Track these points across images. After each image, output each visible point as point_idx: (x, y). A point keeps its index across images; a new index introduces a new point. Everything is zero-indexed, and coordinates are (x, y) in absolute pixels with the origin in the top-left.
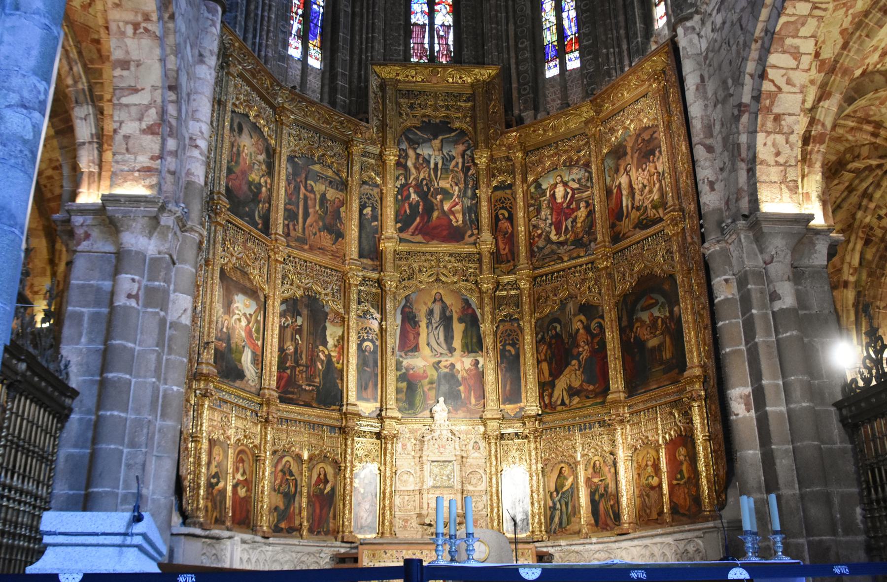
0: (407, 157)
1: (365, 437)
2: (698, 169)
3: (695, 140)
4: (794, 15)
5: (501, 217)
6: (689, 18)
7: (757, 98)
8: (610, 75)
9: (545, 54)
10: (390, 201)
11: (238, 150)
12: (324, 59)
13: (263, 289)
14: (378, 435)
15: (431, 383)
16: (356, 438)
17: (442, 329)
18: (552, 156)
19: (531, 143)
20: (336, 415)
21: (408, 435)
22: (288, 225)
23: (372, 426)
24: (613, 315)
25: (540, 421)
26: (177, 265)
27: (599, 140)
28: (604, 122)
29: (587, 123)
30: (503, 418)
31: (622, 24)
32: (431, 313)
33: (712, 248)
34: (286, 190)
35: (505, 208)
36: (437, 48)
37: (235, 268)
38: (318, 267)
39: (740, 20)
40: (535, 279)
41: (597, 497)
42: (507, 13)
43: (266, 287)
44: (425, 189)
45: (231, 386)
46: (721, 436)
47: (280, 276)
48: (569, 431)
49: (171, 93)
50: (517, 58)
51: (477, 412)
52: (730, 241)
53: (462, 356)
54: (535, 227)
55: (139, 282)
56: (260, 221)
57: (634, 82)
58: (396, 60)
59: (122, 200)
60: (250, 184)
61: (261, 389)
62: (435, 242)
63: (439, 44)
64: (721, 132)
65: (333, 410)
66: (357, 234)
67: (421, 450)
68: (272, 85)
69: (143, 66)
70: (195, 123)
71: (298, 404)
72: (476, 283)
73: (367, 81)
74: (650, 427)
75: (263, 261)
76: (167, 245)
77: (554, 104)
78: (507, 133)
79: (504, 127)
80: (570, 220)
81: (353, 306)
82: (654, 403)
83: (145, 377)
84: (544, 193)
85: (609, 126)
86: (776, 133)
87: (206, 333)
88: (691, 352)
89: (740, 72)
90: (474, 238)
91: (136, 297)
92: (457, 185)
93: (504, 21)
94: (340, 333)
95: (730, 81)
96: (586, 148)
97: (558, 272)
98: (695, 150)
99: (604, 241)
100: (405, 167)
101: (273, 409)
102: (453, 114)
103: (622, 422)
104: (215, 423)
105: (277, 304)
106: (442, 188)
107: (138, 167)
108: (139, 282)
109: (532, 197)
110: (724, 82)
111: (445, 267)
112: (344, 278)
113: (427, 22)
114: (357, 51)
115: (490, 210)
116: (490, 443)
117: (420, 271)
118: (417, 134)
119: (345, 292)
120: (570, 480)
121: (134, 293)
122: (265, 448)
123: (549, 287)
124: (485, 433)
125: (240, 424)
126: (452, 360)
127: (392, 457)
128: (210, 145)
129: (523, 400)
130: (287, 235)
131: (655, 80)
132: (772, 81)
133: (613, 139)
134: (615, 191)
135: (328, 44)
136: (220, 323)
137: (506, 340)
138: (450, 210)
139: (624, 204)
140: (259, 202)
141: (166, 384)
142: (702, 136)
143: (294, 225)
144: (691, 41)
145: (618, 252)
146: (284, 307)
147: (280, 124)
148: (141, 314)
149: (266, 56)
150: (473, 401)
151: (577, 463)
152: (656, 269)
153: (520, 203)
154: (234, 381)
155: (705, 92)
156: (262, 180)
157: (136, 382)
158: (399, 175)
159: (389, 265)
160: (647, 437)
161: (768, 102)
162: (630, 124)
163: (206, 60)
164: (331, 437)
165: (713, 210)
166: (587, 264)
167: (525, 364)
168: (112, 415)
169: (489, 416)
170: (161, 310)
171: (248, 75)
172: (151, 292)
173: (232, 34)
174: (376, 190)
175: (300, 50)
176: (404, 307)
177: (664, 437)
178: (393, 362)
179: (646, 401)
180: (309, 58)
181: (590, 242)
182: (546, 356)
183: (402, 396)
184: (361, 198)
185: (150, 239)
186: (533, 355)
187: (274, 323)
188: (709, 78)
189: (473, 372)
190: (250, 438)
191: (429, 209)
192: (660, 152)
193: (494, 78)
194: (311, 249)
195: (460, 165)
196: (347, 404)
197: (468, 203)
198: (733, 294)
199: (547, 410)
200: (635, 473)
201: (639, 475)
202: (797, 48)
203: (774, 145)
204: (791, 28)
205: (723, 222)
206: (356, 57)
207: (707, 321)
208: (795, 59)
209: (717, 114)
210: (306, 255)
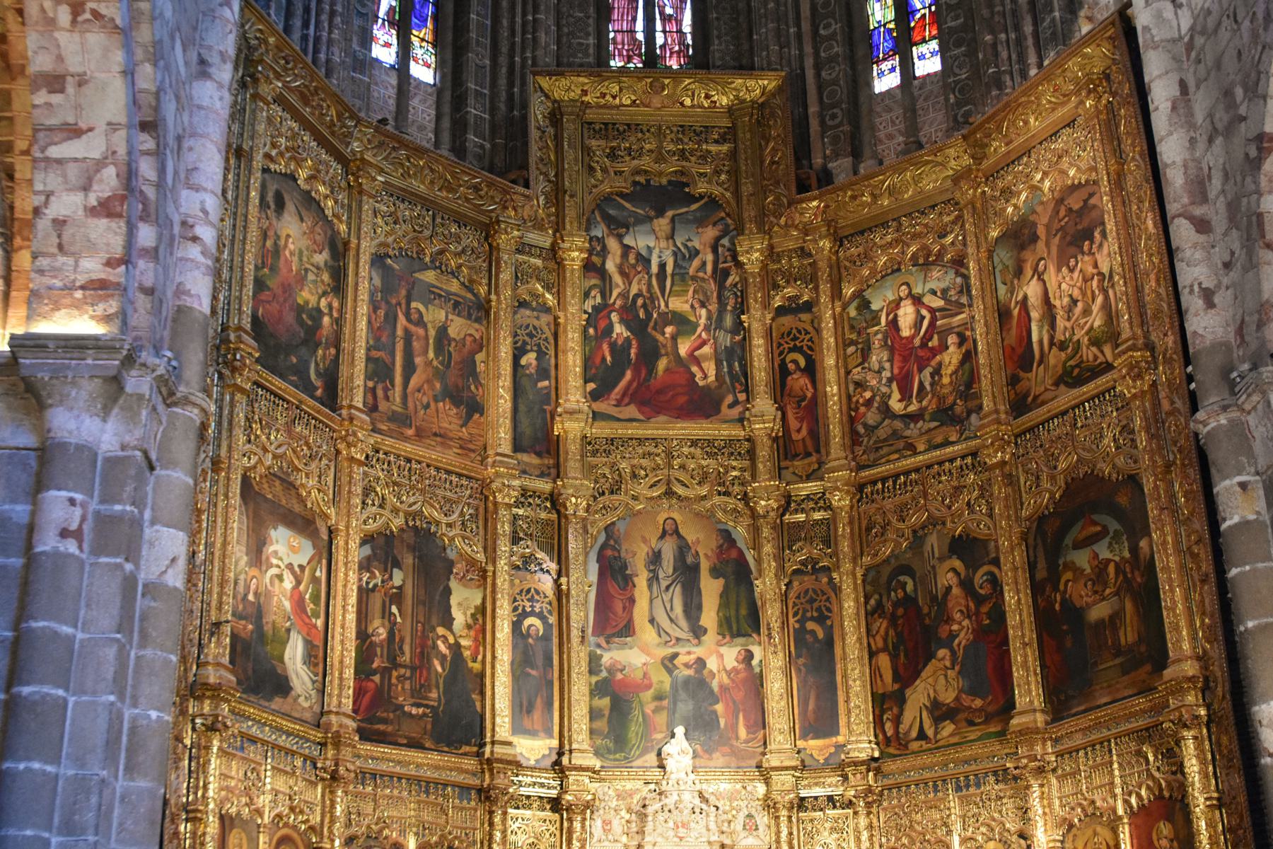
0: (604, 252)
1: (529, 807)
2: (1179, 266)
3: (1172, 208)
5: (791, 366)
8: (1000, 86)
9: (872, 48)
10: (572, 339)
11: (275, 244)
12: (440, 66)
13: (326, 517)
14: (555, 804)
15: (659, 697)
16: (510, 810)
17: (678, 589)
18: (890, 245)
19: (846, 221)
20: (470, 763)
21: (614, 804)
22: (373, 390)
23: (542, 785)
24: (1019, 556)
25: (878, 771)
27: (983, 211)
28: (991, 176)
29: (957, 179)
30: (804, 767)
33: (1211, 421)
34: (369, 322)
35: (799, 350)
36: (660, 39)
37: (271, 476)
38: (433, 472)
40: (861, 488)
43: (332, 512)
44: (642, 314)
45: (263, 709)
46: (1242, 799)
47: (359, 491)
48: (936, 790)
49: (144, 137)
50: (816, 54)
51: (752, 755)
52: (1247, 407)
53: (719, 644)
54: (860, 385)
55: (84, 505)
56: (318, 383)
57: (1048, 98)
58: (581, 65)
59: (51, 345)
60: (300, 309)
61: (322, 714)
62: (662, 418)
63: (664, 31)
65: (465, 754)
66: (509, 405)
67: (641, 832)
68: (340, 116)
69: (91, 85)
70: (193, 194)
72: (745, 498)
73: (525, 106)
75: (325, 461)
76: (138, 433)
77: (892, 144)
78: (802, 201)
79: (794, 189)
80: (927, 372)
81: (504, 546)
82: (1105, 733)
83: (94, 693)
85: (1000, 184)
87: (214, 603)
88: (1177, 629)
89: (1259, 73)
90: (739, 409)
91: (78, 535)
92: (703, 305)
94: (478, 602)
95: (1239, 92)
96: (957, 228)
97: (907, 473)
98: (1172, 229)
99: (997, 411)
100: (602, 273)
101: (346, 753)
102: (694, 167)
103: (1040, 771)
104: (233, 783)
105: (353, 545)
106: (674, 313)
107: (81, 279)
108: (84, 505)
109: (852, 327)
110: (1228, 93)
111: (683, 467)
112: (483, 491)
114: (505, 49)
115: (770, 353)
116: (777, 818)
117: (634, 476)
118: (623, 208)
119: (486, 520)
121: (74, 526)
122: (331, 832)
123: (888, 504)
124: (767, 797)
125: (282, 784)
126: (699, 651)
128: (221, 235)
129: (843, 730)
130: (372, 409)
131: (1089, 92)
133: (1010, 210)
134: (1016, 312)
135: (449, 36)
136: (241, 583)
137: (805, 611)
138: (691, 354)
139: (1035, 337)
140: (318, 345)
141: (135, 705)
142: (1186, 200)
143: (386, 390)
144: (1159, 16)
145: (1024, 433)
146: (367, 550)
147: (355, 191)
148: (87, 568)
149: (328, 61)
150: (743, 732)
152: (1100, 465)
153: (829, 339)
154: (270, 700)
155: (1190, 114)
156: (323, 302)
157: (76, 703)
158: (591, 288)
159: (572, 466)
160: (1093, 802)
162: (1042, 179)
163: (212, 70)
164: (462, 809)
166: (963, 457)
167: (844, 658)
168: (28, 770)
169: (775, 763)
170: (127, 560)
171: (293, 99)
172: (105, 523)
173: (261, 19)
174: (545, 319)
175: (394, 49)
176: (603, 547)
177: (1126, 802)
178: (584, 656)
179: (1088, 728)
180: (412, 63)
181: (969, 413)
182: (885, 640)
183: (602, 724)
184: (516, 335)
185: (104, 420)
186: (859, 639)
187: (348, 582)
188: (1198, 87)
190: (302, 812)
191: (650, 353)
192: (1104, 234)
193: (773, 95)
194: (420, 435)
195: (709, 268)
196: (493, 743)
197: (726, 340)
198: (1258, 513)
199: (891, 750)
205: (1232, 370)
206: (503, 60)
207: (1207, 566)
209: (1215, 157)
210: (408, 448)
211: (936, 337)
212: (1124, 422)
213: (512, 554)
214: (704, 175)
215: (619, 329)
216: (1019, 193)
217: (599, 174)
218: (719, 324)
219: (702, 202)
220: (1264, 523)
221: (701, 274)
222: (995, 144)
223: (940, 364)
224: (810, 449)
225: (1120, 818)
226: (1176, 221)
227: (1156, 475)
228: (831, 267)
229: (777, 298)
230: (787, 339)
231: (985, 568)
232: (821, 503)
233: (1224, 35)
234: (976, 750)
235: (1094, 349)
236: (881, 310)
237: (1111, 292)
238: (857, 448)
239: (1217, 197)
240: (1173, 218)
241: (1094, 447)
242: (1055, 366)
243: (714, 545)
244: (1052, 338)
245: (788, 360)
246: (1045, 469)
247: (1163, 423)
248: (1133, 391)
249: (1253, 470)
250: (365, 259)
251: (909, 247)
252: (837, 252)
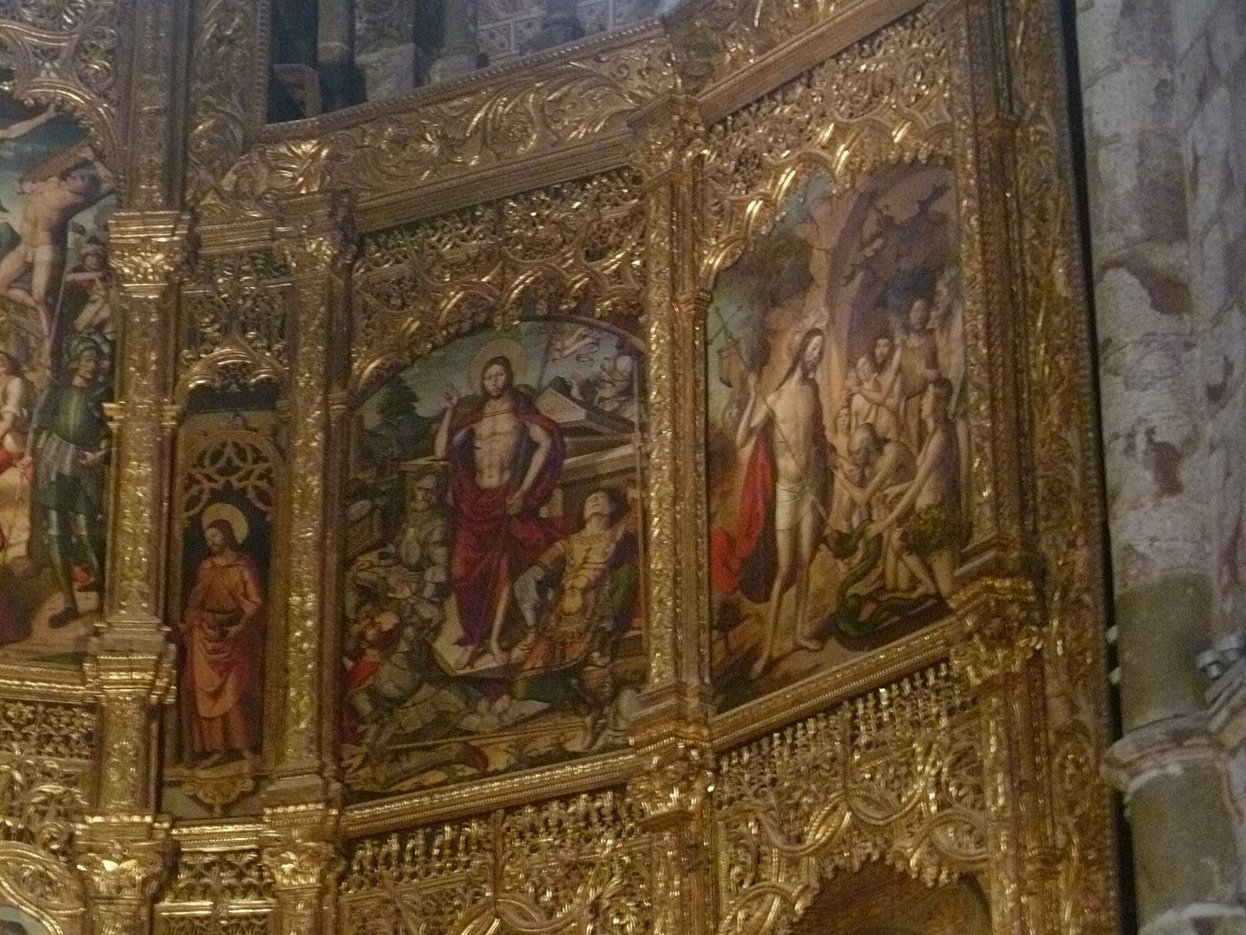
2: (1111, 385)
3: (1106, 244)
5: (214, 536)
18: (475, 264)
29: (639, 122)
40: (347, 846)
52: (1231, 739)
54: (372, 596)
64: (1220, 217)
72: (69, 850)
79: (260, 110)
80: (536, 573)
90: (75, 630)
97: (459, 820)
99: (679, 689)
115: (164, 497)
123: (410, 894)
133: (754, 207)
134: (745, 453)
139: (783, 519)
145: (737, 747)
152: (905, 843)
162: (832, 144)
165: (1165, 584)
181: (618, 686)
195: (40, 279)
205: (1206, 645)
211: (558, 495)
212: (963, 744)
214: (51, 54)
216: (779, 170)
219: (41, 119)
221: (18, 294)
222: (735, 47)
223: (562, 561)
224: (239, 741)
226: (1110, 274)
227: (1020, 881)
228: (331, 304)
229: (196, 368)
230: (210, 470)
232: (252, 877)
235: (912, 561)
236: (439, 419)
237: (961, 429)
238: (348, 749)
239: (1207, 231)
240: (1104, 269)
241: (891, 796)
242: (822, 592)
244: (820, 523)
245: (207, 520)
246: (777, 839)
247: (1050, 754)
248: (988, 672)
249: (1230, 890)
251: (517, 272)
252: (349, 268)
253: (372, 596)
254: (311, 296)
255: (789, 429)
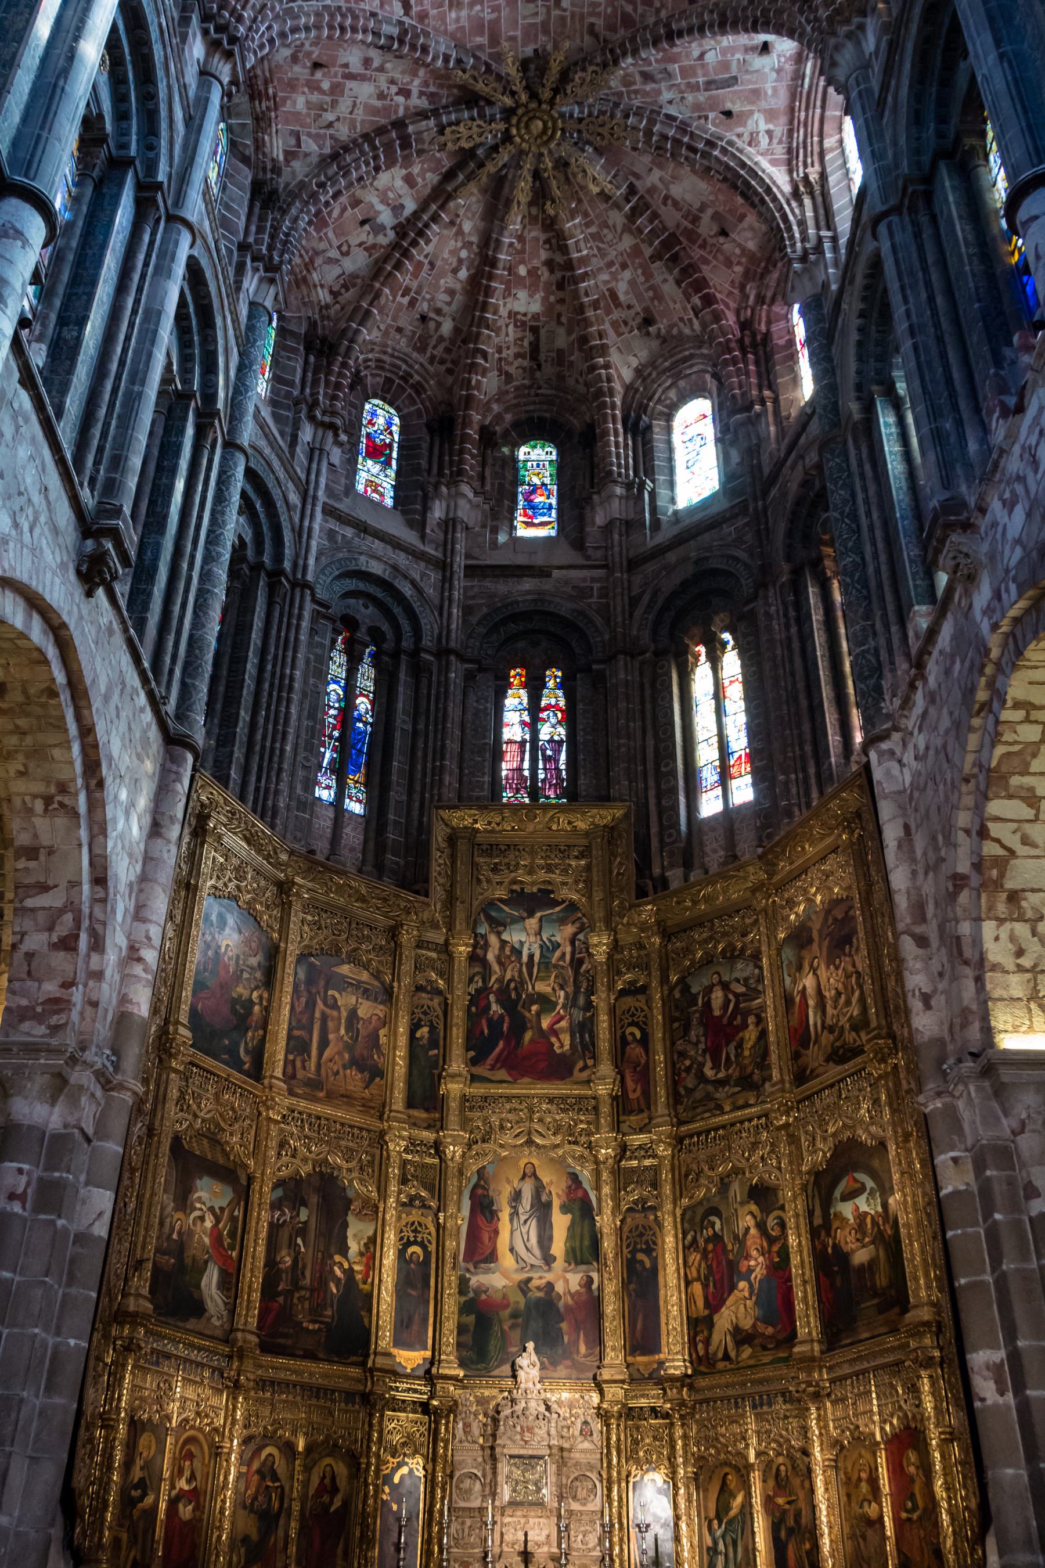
0: (486, 946)
3: (901, 926)
4: (1016, 742)
5: (630, 1038)
6: (885, 736)
7: (978, 866)
10: (458, 1015)
13: (246, 1166)
15: (515, 1315)
17: (533, 1224)
18: (706, 941)
22: (293, 1061)
23: (415, 1391)
25: (691, 1387)
26: (96, 1143)
27: (773, 917)
28: (780, 888)
29: (754, 890)
31: (808, 736)
32: (517, 1196)
35: (635, 1024)
36: (541, 776)
37: (200, 1134)
39: (945, 746)
40: (680, 1140)
41: (783, 1534)
42: (643, 720)
43: (251, 1163)
48: (737, 1407)
49: (98, 889)
53: (566, 1271)
57: (817, 831)
60: (235, 1002)
62: (526, 1080)
67: (494, 1436)
71: (292, 1355)
72: (590, 1146)
73: (429, 832)
74: (861, 1409)
76: (76, 1115)
79: (633, 894)
81: (393, 1188)
82: (866, 1365)
84: (693, 1000)
86: (1013, 920)
88: (916, 1279)
92: (562, 988)
93: (639, 733)
94: (371, 1233)
95: (940, 838)
97: (716, 1129)
99: (782, 1081)
103: (817, 1397)
106: (539, 994)
109: (677, 1007)
110: (934, 838)
111: (541, 1120)
113: (527, 737)
117: (502, 1127)
120: (739, 1499)
123: (702, 1155)
124: (599, 1408)
126: (549, 1277)
127: (446, 1448)
130: (289, 1076)
132: (998, 841)
135: (376, 779)
138: (551, 1027)
142: (908, 921)
143: (303, 1061)
146: (280, 1192)
150: (583, 1349)
151: (749, 1467)
152: (860, 1132)
155: (912, 850)
156: (255, 994)
159: (453, 1118)
161: (995, 873)
174: (437, 1001)
177: (882, 1429)
179: (854, 1360)
183: (468, 1339)
185: (53, 1105)
186: (678, 1270)
187: (262, 1220)
189: (584, 1298)
191: (519, 1025)
193: (620, 821)
194: (331, 1097)
195: (568, 957)
197: (579, 1016)
199: (703, 1369)
200: (842, 1492)
201: (848, 1495)
202: (1032, 789)
203: (1012, 938)
204: (1016, 762)
206: (417, 797)
208: (1031, 806)
209: (928, 887)
210: (318, 1109)
213: (400, 1192)
214: (564, 884)
215: (495, 1007)
217: (485, 885)
218: (574, 1004)
220: (972, 1193)
225: (878, 1444)
231: (776, 1213)
233: (930, 792)
234: (768, 1373)
243: (564, 1185)
244: (823, 1022)
250: (291, 959)
253: (682, 1055)
254: (654, 956)
255: (811, 991)
